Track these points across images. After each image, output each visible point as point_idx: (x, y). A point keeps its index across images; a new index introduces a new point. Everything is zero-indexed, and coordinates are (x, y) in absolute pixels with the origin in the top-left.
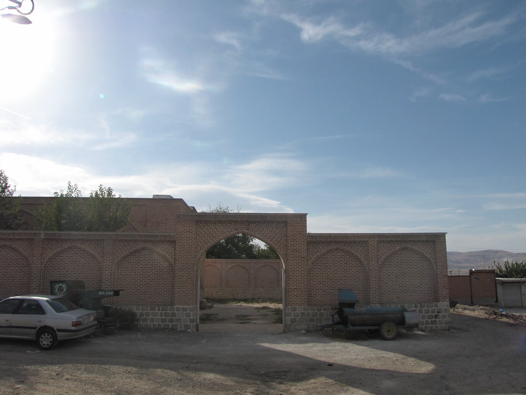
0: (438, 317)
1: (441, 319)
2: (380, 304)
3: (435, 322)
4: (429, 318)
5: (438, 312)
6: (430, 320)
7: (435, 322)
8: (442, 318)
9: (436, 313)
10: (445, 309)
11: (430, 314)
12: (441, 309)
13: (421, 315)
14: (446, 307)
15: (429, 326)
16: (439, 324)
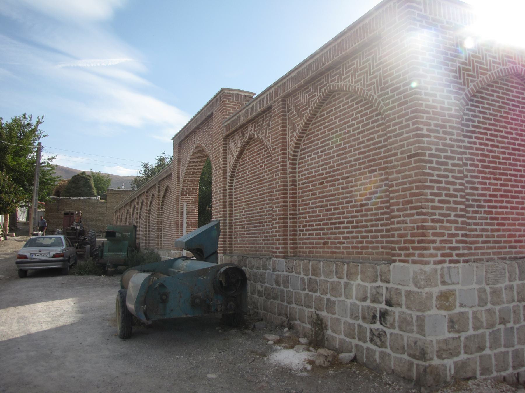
0: (390, 319)
1: (397, 331)
2: (284, 257)
3: (381, 335)
4: (364, 318)
5: (389, 303)
6: (368, 326)
7: (381, 335)
8: (401, 329)
9: (383, 306)
10: (409, 293)
11: (368, 303)
12: (398, 293)
13: (349, 301)
14: (412, 288)
15: (365, 345)
16: (391, 349)
